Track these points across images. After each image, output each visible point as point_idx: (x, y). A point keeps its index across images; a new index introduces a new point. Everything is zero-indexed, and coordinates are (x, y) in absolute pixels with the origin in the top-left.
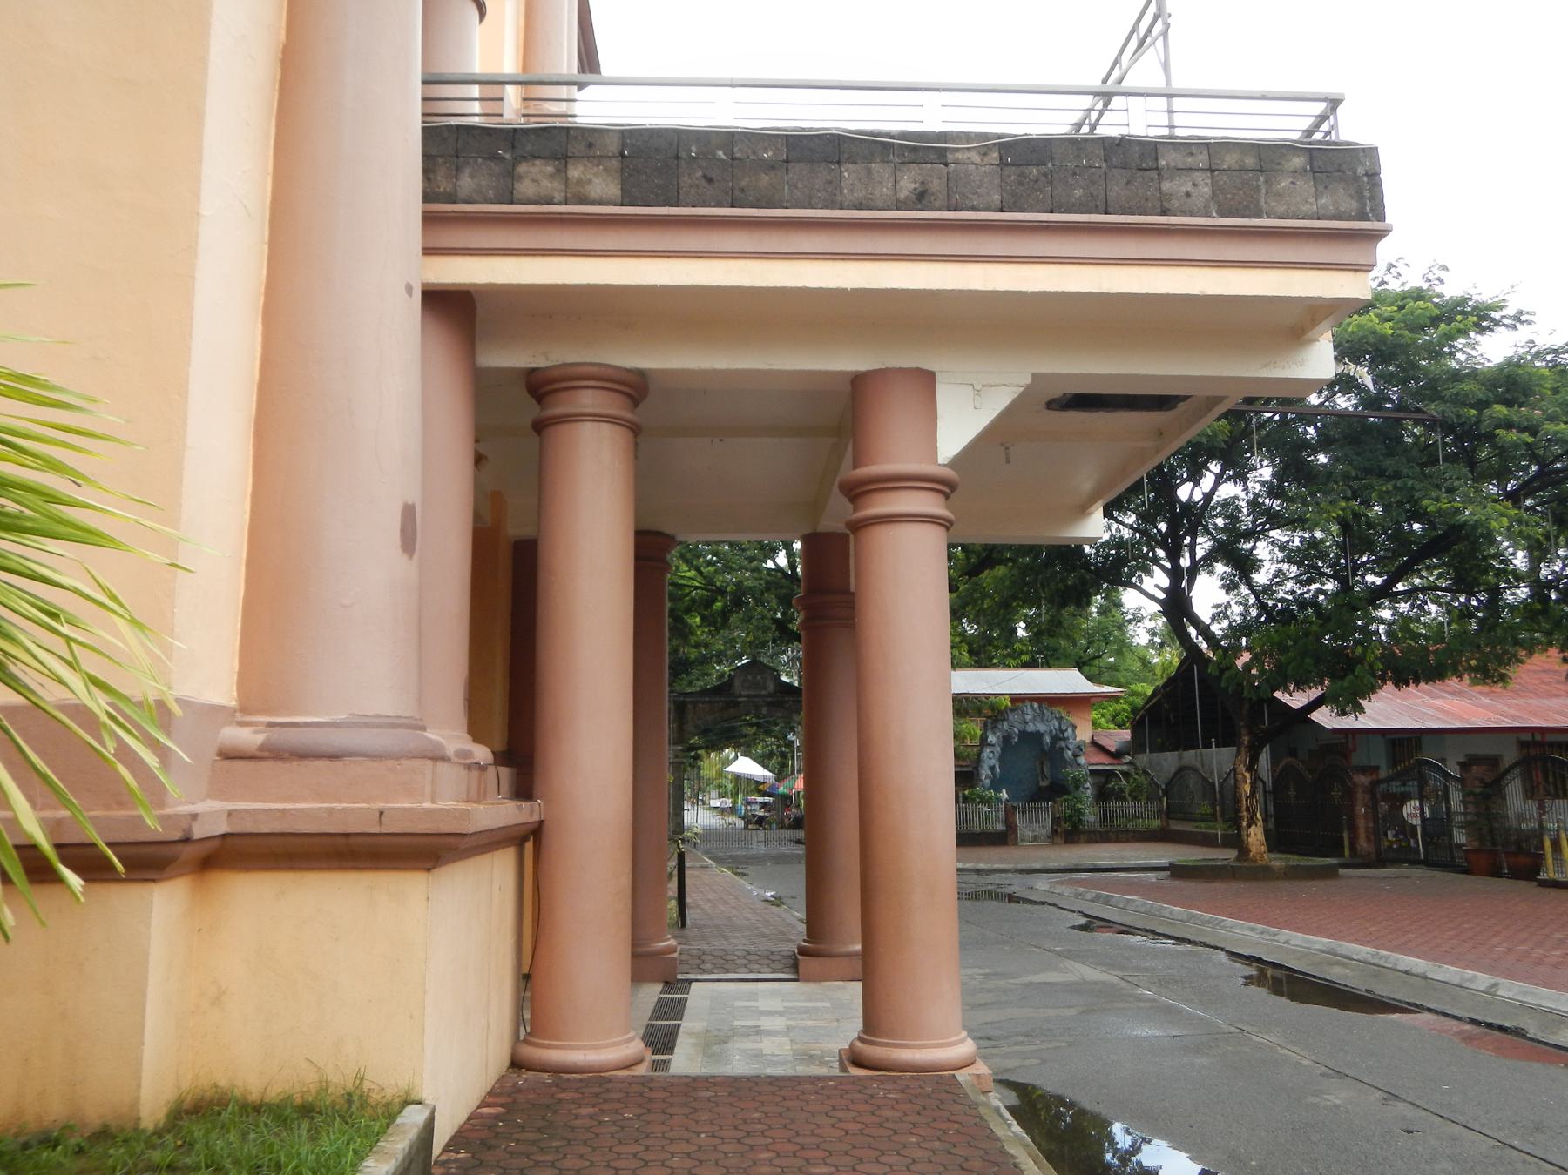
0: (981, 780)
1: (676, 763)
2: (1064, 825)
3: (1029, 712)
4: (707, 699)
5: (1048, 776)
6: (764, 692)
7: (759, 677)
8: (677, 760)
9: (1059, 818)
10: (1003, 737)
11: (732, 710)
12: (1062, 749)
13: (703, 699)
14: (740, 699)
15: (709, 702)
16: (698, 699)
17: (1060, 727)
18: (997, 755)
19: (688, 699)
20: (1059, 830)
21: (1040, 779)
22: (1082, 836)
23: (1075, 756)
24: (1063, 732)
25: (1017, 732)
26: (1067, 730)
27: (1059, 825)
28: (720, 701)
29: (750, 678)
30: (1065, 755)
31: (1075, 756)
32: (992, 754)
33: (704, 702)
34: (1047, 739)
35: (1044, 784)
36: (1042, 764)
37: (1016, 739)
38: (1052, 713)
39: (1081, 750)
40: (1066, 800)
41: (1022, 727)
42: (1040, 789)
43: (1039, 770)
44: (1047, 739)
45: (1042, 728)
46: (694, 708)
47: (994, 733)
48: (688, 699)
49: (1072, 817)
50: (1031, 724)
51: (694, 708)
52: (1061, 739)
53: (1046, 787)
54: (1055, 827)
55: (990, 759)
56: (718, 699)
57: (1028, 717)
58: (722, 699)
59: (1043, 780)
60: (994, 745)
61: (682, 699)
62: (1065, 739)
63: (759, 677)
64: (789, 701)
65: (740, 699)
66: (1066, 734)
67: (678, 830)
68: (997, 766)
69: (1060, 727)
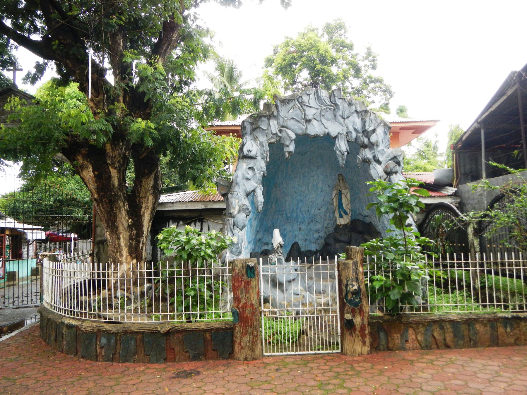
0: (231, 215)
2: (367, 307)
3: (313, 102)
5: (348, 211)
9: (357, 293)
10: (270, 144)
12: (366, 161)
17: (364, 125)
18: (259, 175)
20: (358, 320)
21: (337, 215)
22: (411, 334)
23: (389, 173)
24: (367, 133)
25: (293, 136)
26: (374, 131)
27: (357, 308)
30: (372, 172)
31: (389, 173)
32: (250, 172)
34: (342, 146)
35: (343, 221)
36: (340, 193)
37: (292, 148)
38: (350, 104)
39: (398, 163)
40: (374, 249)
41: (300, 128)
42: (337, 228)
43: (335, 203)
44: (342, 146)
45: (334, 129)
47: (255, 139)
49: (388, 289)
50: (314, 122)
52: (365, 146)
53: (345, 226)
54: (348, 316)
55: (248, 179)
57: (310, 113)
59: (341, 216)
60: (252, 158)
62: (371, 146)
66: (373, 138)
68: (259, 192)
69: (364, 125)
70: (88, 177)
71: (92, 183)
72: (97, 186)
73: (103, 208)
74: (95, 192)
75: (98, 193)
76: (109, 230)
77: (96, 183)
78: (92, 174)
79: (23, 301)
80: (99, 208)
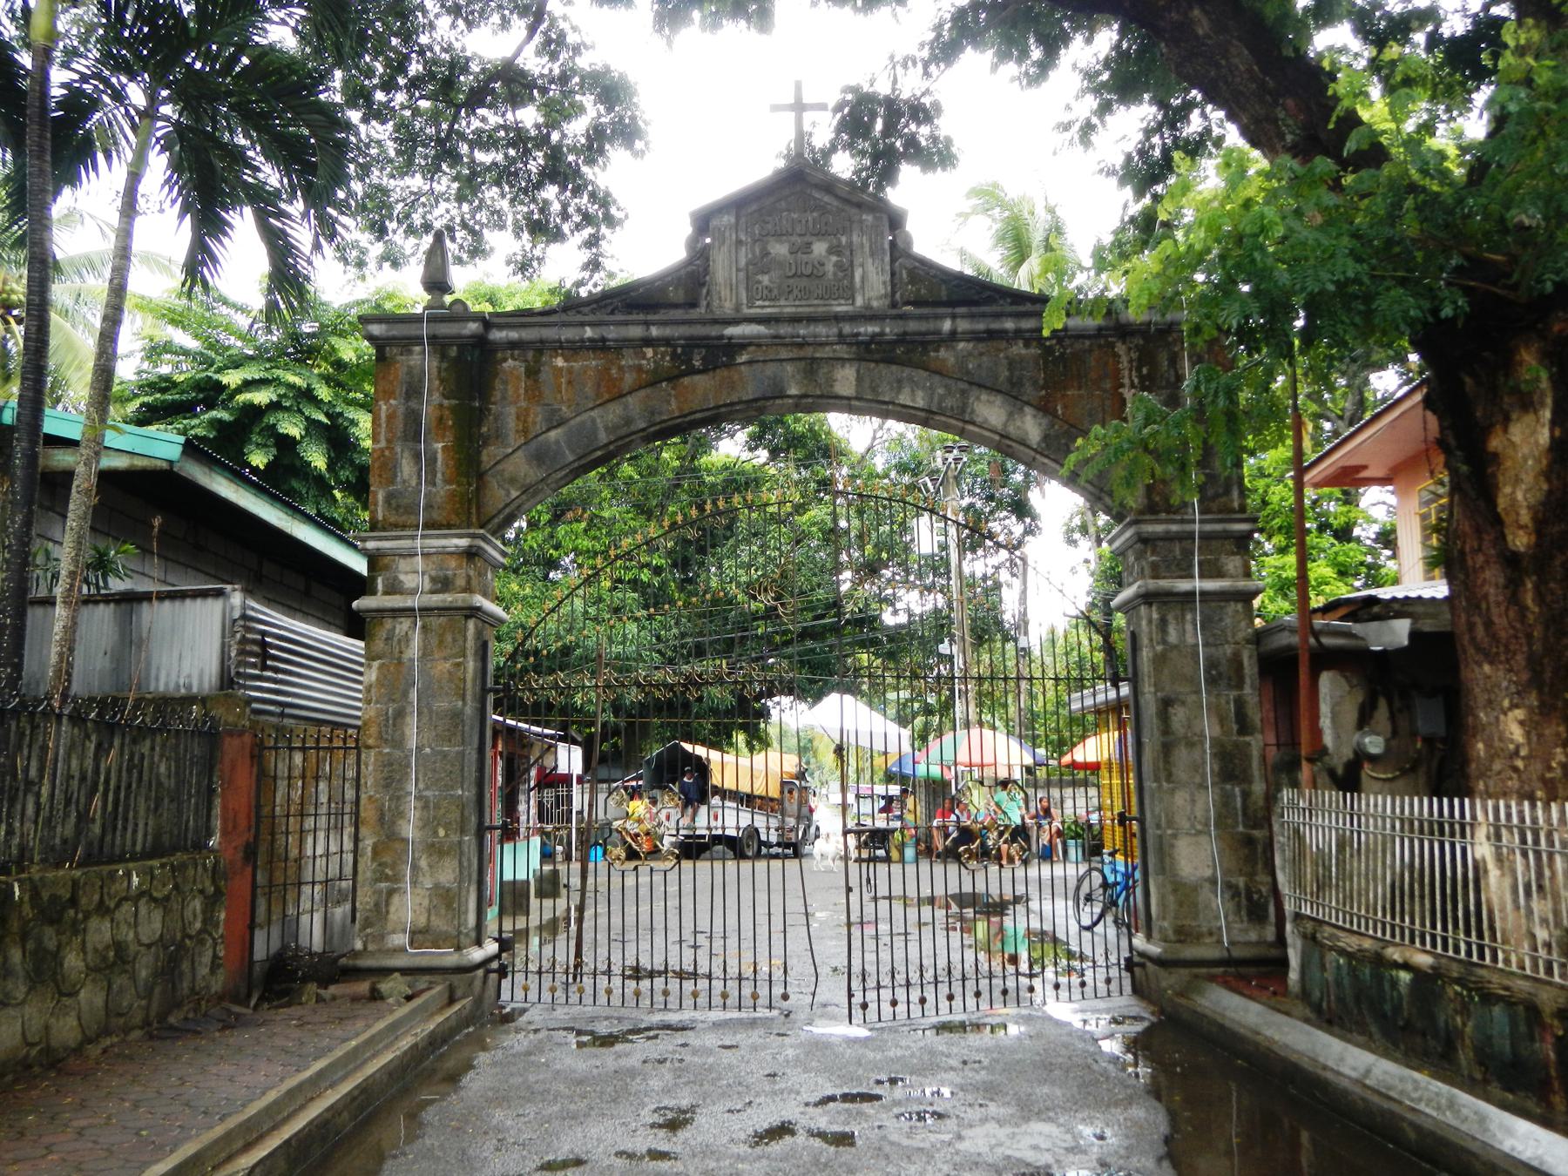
4: (589, 332)
6: (841, 308)
7: (820, 248)
8: (447, 598)
11: (701, 381)
13: (568, 334)
14: (731, 331)
15: (599, 346)
16: (549, 333)
28: (648, 342)
29: (780, 249)
33: (574, 349)
46: (532, 372)
51: (532, 372)
56: (636, 332)
58: (655, 331)
63: (820, 248)
64: (953, 336)
65: (731, 331)
67: (440, 924)
70: (1525, 450)
71: (1528, 478)
72: (1550, 492)
73: (1540, 597)
74: (1525, 517)
75: (1541, 524)
76: (1533, 699)
77: (1548, 480)
78: (1544, 436)
79: (894, 1003)
80: (1514, 599)
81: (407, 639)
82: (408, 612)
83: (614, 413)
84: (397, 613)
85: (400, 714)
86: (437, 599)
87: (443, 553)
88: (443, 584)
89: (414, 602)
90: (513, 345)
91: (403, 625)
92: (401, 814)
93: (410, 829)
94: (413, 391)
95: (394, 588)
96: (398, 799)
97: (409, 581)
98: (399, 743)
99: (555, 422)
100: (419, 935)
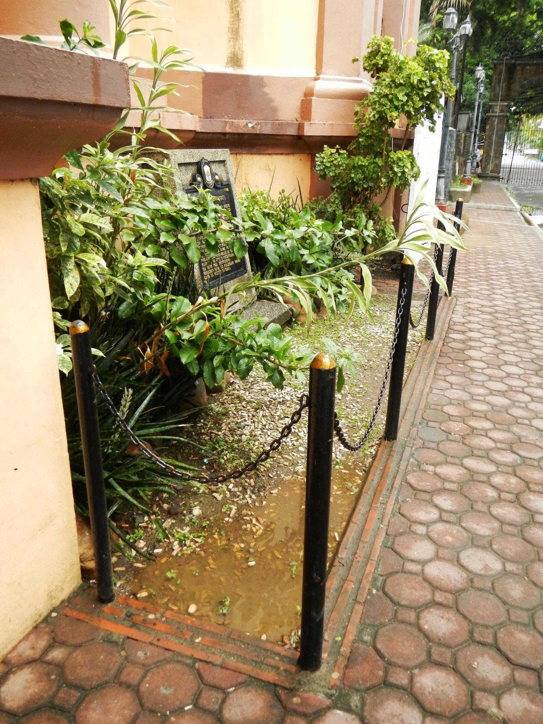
1: (502, 116)
13: (531, 62)
15: (536, 64)
16: (527, 62)
19: (518, 62)
33: (531, 65)
46: (523, 69)
48: (518, 62)
51: (523, 69)
61: (513, 61)
67: (495, 170)
81: (495, 121)
82: (496, 116)
83: (537, 77)
84: (493, 116)
85: (492, 134)
86: (501, 114)
87: (503, 105)
88: (502, 111)
89: (497, 114)
90: (520, 64)
91: (494, 119)
92: (491, 151)
93: (492, 154)
94: (500, 73)
95: (493, 112)
96: (491, 149)
97: (496, 110)
98: (491, 139)
99: (525, 79)
100: (492, 172)
